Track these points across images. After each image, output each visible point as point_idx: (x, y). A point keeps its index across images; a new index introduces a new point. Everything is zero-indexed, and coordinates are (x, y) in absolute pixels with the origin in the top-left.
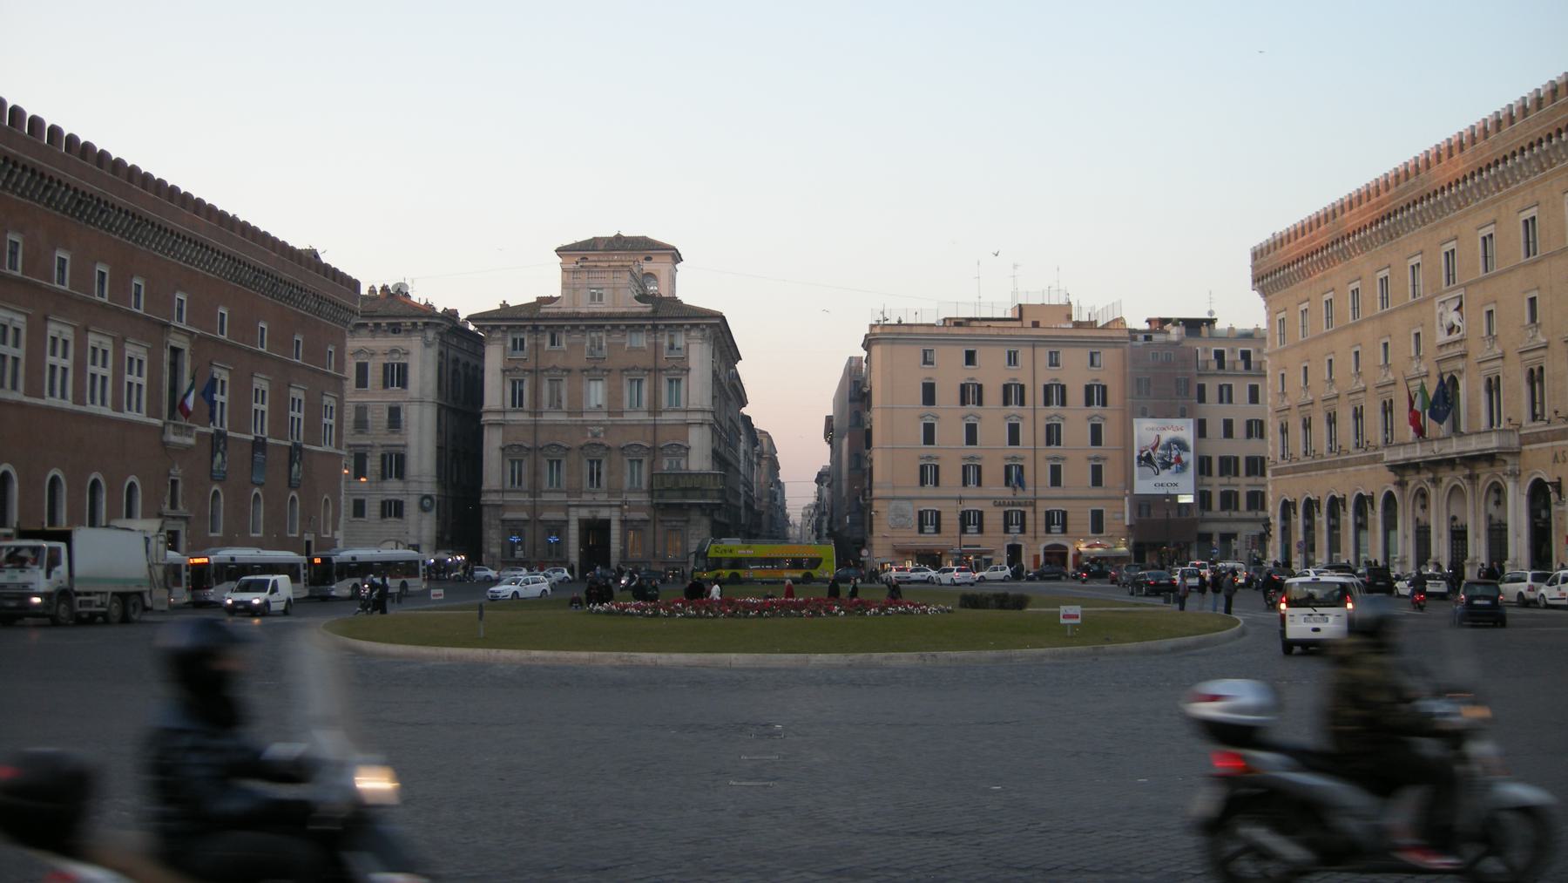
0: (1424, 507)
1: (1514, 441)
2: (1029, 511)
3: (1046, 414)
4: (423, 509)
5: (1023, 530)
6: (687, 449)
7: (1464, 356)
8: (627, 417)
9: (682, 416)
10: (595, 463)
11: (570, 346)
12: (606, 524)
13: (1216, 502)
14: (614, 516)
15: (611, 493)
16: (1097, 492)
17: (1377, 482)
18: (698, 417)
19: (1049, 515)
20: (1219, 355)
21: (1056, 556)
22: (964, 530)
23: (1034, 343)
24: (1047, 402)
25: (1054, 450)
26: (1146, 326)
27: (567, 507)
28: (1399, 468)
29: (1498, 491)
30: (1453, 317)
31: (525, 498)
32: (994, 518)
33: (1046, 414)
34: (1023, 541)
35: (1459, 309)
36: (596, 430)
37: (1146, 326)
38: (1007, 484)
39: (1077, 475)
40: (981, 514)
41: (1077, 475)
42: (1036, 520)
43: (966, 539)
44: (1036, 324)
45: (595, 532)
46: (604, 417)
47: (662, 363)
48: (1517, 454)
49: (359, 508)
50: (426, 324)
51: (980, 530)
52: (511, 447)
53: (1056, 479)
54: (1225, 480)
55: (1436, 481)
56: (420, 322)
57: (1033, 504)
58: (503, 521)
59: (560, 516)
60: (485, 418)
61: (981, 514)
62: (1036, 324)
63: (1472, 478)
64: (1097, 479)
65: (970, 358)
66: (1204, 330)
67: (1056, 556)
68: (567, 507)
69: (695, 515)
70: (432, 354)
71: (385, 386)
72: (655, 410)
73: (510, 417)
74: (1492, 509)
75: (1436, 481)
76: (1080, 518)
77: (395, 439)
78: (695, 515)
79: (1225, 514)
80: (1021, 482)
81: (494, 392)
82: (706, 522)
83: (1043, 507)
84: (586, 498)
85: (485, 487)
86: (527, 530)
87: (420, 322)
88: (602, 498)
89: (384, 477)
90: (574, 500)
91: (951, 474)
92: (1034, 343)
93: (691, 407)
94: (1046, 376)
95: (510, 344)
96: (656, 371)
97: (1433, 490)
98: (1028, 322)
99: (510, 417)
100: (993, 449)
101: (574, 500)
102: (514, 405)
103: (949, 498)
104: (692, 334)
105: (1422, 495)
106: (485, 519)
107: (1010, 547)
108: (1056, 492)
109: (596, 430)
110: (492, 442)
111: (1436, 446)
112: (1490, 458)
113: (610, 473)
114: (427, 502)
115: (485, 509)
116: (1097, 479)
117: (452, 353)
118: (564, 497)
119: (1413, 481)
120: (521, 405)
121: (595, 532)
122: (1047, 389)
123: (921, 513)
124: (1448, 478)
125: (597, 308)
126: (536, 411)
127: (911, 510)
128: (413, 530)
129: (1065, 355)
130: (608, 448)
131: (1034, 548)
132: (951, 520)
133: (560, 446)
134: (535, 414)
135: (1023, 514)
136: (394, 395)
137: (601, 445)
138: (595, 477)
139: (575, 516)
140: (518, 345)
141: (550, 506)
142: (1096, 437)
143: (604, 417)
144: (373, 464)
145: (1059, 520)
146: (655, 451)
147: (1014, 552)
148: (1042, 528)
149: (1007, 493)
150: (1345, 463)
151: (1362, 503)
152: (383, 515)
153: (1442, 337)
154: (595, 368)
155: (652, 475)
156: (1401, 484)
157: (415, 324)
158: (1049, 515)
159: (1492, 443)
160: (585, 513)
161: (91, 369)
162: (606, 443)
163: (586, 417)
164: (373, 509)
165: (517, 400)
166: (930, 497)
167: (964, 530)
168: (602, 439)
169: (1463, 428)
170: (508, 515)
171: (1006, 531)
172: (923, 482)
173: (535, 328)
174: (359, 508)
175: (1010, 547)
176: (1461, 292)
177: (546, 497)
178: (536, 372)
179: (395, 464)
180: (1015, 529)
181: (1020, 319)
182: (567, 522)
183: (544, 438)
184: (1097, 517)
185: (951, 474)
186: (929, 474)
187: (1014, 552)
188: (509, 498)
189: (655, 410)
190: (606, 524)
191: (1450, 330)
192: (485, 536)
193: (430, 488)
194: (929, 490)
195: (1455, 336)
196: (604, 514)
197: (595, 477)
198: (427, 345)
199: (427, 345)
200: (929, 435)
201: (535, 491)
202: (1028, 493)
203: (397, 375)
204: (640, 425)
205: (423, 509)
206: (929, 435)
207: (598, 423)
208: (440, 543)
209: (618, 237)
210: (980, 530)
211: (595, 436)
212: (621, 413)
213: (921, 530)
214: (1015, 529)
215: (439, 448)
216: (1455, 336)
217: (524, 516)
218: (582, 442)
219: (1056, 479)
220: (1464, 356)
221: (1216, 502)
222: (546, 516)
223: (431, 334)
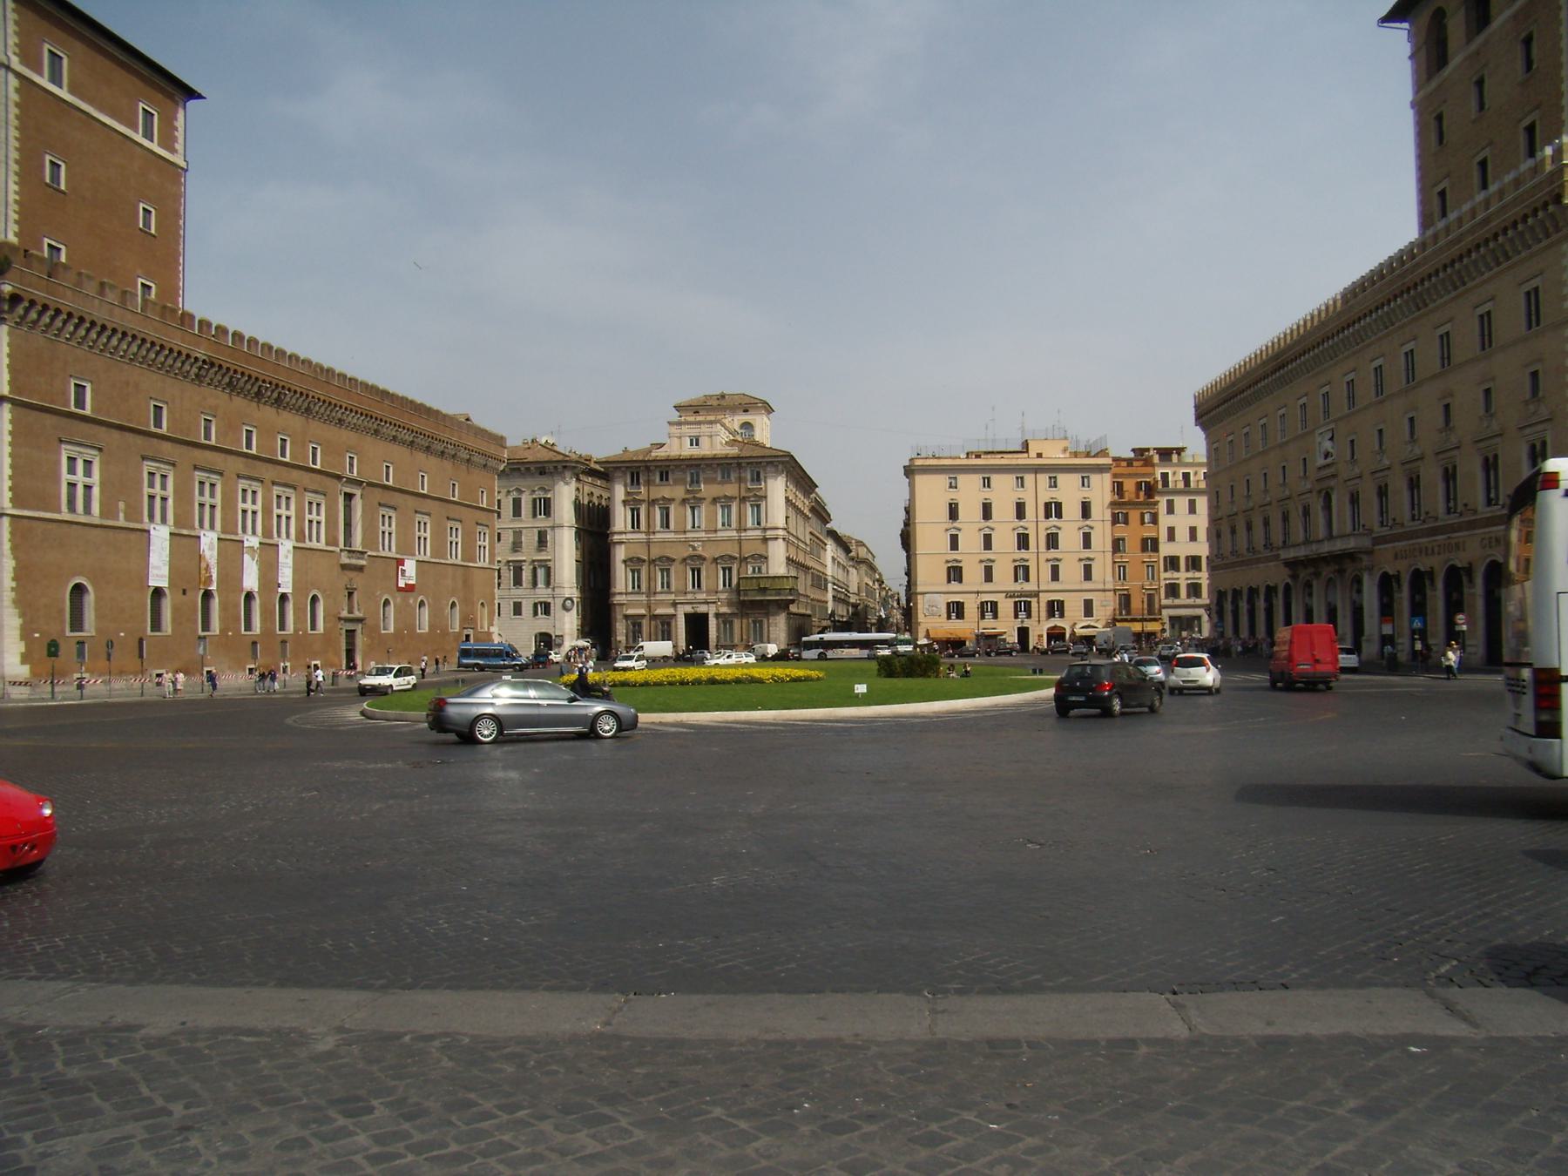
0: (1310, 595)
1: (1366, 542)
2: (1034, 601)
3: (1047, 525)
4: (565, 608)
5: (1029, 616)
7: (1334, 476)
9: (758, 533)
10: (697, 572)
12: (705, 616)
13: (1183, 591)
15: (708, 592)
16: (1088, 585)
17: (1276, 575)
19: (1051, 604)
20: (1186, 476)
21: (1056, 635)
22: (983, 617)
23: (1037, 470)
24: (1048, 515)
25: (1053, 553)
26: (1132, 455)
27: (674, 604)
28: (1292, 564)
29: (1358, 581)
30: (1328, 445)
32: (1006, 607)
33: (1047, 525)
35: (1331, 439)
37: (1132, 455)
39: (1071, 572)
41: (1071, 572)
42: (1039, 607)
43: (983, 623)
44: (1039, 455)
48: (1370, 553)
49: (518, 609)
51: (995, 616)
52: (631, 560)
53: (1055, 575)
54: (1190, 575)
55: (1317, 575)
58: (626, 617)
59: (671, 611)
62: (1039, 455)
63: (1341, 572)
64: (1088, 575)
65: (987, 483)
66: (1175, 457)
67: (1056, 635)
68: (674, 604)
71: (535, 515)
72: (739, 530)
73: (630, 536)
74: (1355, 596)
75: (1317, 575)
76: (1074, 606)
79: (1191, 601)
80: (1027, 579)
81: (621, 519)
83: (1045, 598)
84: (689, 597)
85: (613, 590)
86: (645, 622)
91: (973, 574)
92: (1037, 470)
94: (1046, 495)
96: (743, 500)
97: (1314, 583)
98: (1033, 453)
101: (681, 598)
105: (1309, 585)
110: (620, 554)
111: (1314, 547)
112: (1351, 556)
113: (707, 577)
114: (568, 603)
116: (1088, 575)
117: (587, 489)
118: (673, 597)
119: (1304, 574)
122: (1047, 506)
124: (1327, 571)
125: (695, 452)
127: (941, 602)
129: (1062, 478)
131: (1039, 630)
132: (971, 609)
134: (648, 533)
136: (542, 522)
138: (697, 584)
139: (682, 611)
140: (635, 480)
142: (1087, 543)
144: (526, 575)
145: (1056, 608)
147: (1023, 633)
148: (1044, 614)
150: (1258, 561)
151: (1271, 591)
153: (1321, 462)
156: (1294, 577)
158: (1051, 604)
159: (1351, 544)
160: (689, 609)
161: (276, 511)
162: (705, 554)
164: (527, 609)
165: (636, 523)
167: (983, 617)
168: (700, 551)
169: (1335, 533)
170: (630, 612)
171: (1016, 617)
173: (648, 468)
174: (518, 609)
176: (1332, 426)
177: (659, 597)
180: (1022, 615)
183: (656, 552)
184: (1088, 608)
186: (955, 573)
187: (1023, 633)
189: (741, 528)
190: (705, 616)
191: (1327, 455)
194: (955, 586)
195: (1329, 460)
196: (702, 609)
197: (697, 584)
200: (954, 543)
201: (651, 592)
202: (1030, 587)
203: (545, 507)
204: (730, 540)
206: (954, 543)
209: (723, 396)
210: (995, 616)
211: (694, 549)
213: (949, 617)
214: (1022, 615)
216: (1329, 460)
217: (643, 611)
219: (1055, 575)
220: (1334, 476)
221: (1183, 591)
222: (659, 611)
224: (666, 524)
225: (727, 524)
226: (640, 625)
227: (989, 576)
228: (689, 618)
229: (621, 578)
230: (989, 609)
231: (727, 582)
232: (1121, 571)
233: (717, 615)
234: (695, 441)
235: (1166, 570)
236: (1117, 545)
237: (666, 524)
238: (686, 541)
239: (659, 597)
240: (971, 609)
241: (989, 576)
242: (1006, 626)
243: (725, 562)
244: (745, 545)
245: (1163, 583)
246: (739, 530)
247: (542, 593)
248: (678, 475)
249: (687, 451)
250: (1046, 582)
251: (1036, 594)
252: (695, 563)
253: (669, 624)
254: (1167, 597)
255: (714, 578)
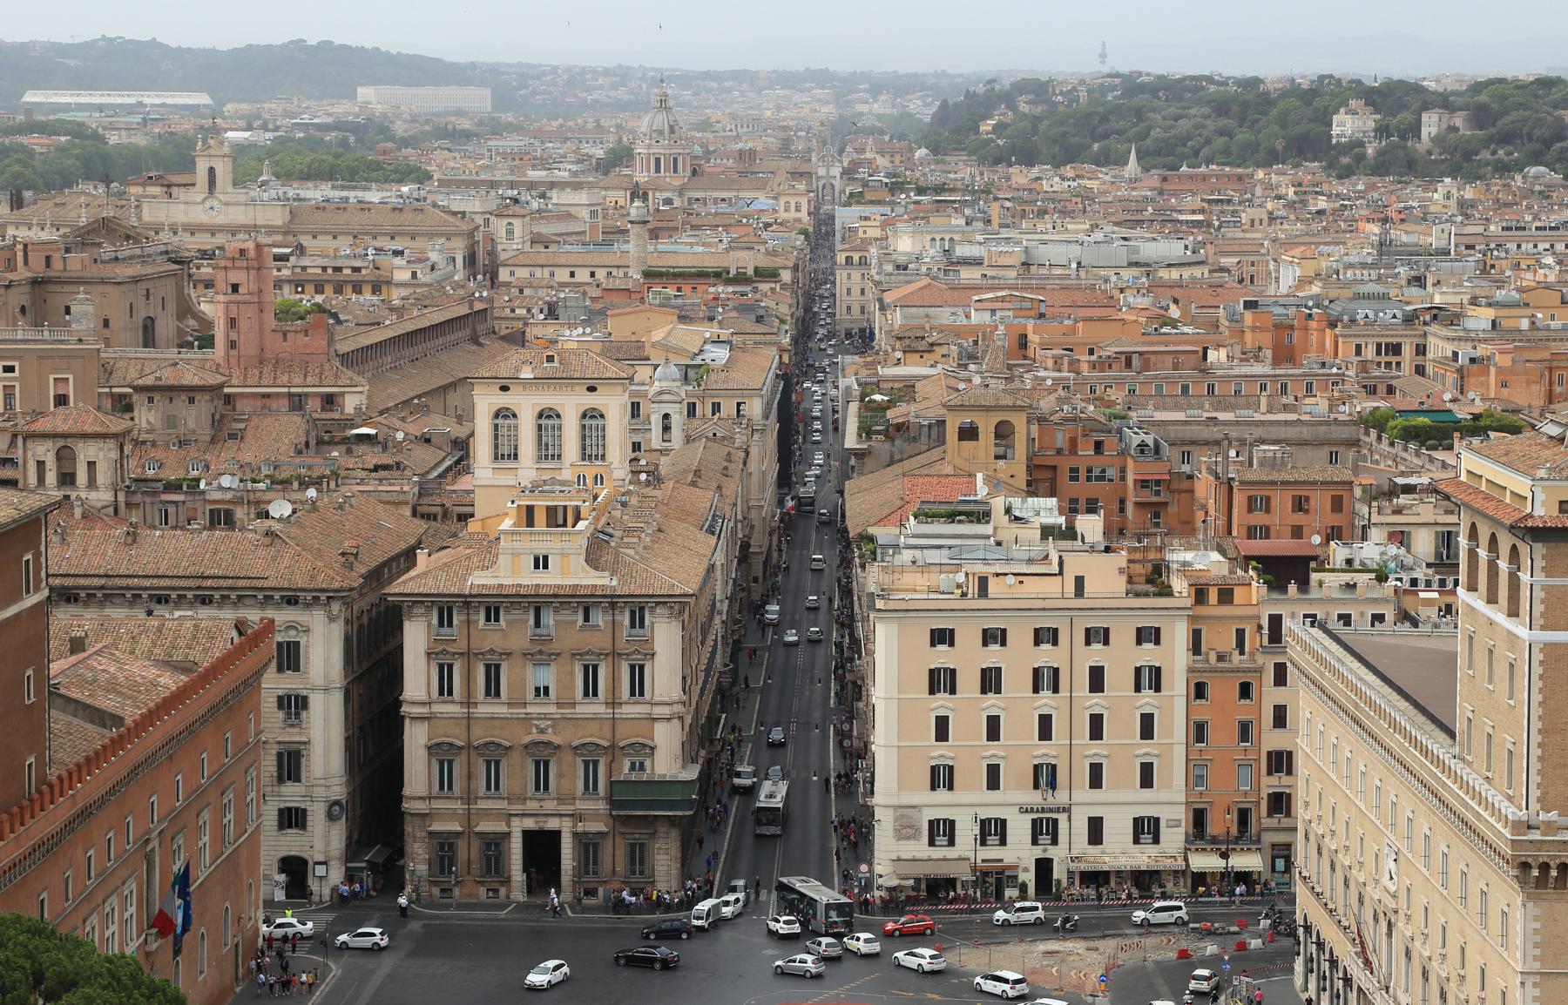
5: (1055, 842)
6: (652, 749)
8: (579, 709)
10: (542, 768)
11: (509, 623)
14: (566, 828)
15: (561, 800)
18: (666, 710)
31: (458, 805)
32: (1020, 828)
34: (1057, 854)
36: (543, 724)
38: (1036, 786)
40: (1004, 822)
45: (542, 847)
46: (552, 709)
47: (621, 645)
50: (329, 598)
52: (438, 745)
53: (1096, 780)
56: (323, 597)
57: (1067, 810)
58: (430, 833)
59: (501, 827)
60: (405, 709)
61: (1004, 822)
62: (1080, 581)
64: (1147, 780)
69: (662, 830)
70: (337, 631)
73: (437, 708)
77: (294, 736)
78: (662, 830)
80: (1052, 785)
81: (417, 680)
82: (675, 833)
84: (532, 806)
85: (407, 791)
87: (323, 597)
88: (550, 805)
89: (281, 780)
90: (516, 808)
91: (971, 775)
93: (657, 699)
95: (435, 621)
99: (437, 708)
100: (1020, 748)
101: (516, 808)
102: (441, 693)
103: (967, 804)
104: (658, 610)
106: (408, 829)
107: (1038, 861)
108: (1096, 795)
109: (543, 724)
110: (415, 740)
113: (560, 776)
115: (408, 818)
116: (1147, 780)
118: (502, 804)
120: (450, 693)
121: (542, 847)
123: (931, 823)
126: (469, 702)
128: (319, 845)
130: (558, 747)
132: (967, 832)
133: (499, 745)
134: (468, 704)
135: (1056, 821)
137: (549, 744)
138: (541, 783)
139: (518, 827)
140: (445, 619)
141: (486, 813)
143: (552, 709)
146: (613, 750)
147: (1044, 867)
149: (1035, 798)
152: (281, 826)
154: (541, 652)
155: (612, 784)
157: (316, 599)
160: (530, 824)
162: (557, 740)
163: (530, 709)
165: (445, 688)
166: (938, 804)
167: (983, 843)
170: (437, 827)
171: (1035, 842)
172: (934, 786)
173: (467, 604)
175: (1038, 861)
177: (482, 805)
178: (468, 655)
179: (291, 764)
180: (1044, 839)
181: (1061, 573)
182: (508, 834)
183: (480, 735)
185: (971, 775)
187: (1044, 867)
188: (437, 804)
192: (408, 849)
193: (339, 791)
194: (942, 795)
196: (552, 824)
197: (541, 783)
198: (332, 619)
199: (332, 619)
200: (942, 729)
201: (469, 797)
202: (1061, 797)
204: (596, 719)
205: (331, 817)
206: (942, 729)
207: (545, 717)
208: (353, 849)
210: (1003, 842)
211: (542, 731)
212: (574, 705)
213: (932, 843)
214: (1044, 839)
215: (347, 739)
218: (527, 739)
219: (1096, 780)
222: (485, 826)
223: (336, 607)
224: (493, 689)
225: (590, 689)
226: (451, 845)
227: (993, 782)
228: (528, 835)
229: (417, 773)
230: (993, 830)
231: (590, 786)
232: (1195, 776)
233: (575, 835)
234: (541, 562)
235: (1270, 773)
236: (1199, 732)
237: (493, 689)
238: (528, 719)
239: (482, 805)
240: (967, 832)
241: (993, 782)
242: (1019, 852)
243: (589, 755)
244: (621, 730)
245: (1264, 794)
246: (614, 703)
247: (292, 794)
248: (516, 614)
249: (531, 579)
250: (1083, 793)
251: (1067, 810)
252: (542, 757)
253: (497, 845)
254: (1270, 815)
255: (568, 775)
